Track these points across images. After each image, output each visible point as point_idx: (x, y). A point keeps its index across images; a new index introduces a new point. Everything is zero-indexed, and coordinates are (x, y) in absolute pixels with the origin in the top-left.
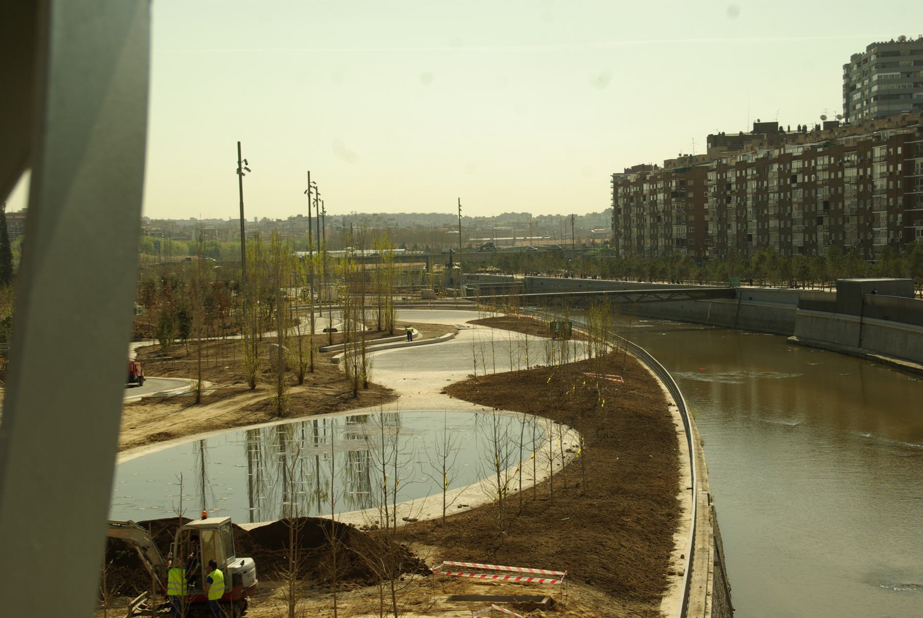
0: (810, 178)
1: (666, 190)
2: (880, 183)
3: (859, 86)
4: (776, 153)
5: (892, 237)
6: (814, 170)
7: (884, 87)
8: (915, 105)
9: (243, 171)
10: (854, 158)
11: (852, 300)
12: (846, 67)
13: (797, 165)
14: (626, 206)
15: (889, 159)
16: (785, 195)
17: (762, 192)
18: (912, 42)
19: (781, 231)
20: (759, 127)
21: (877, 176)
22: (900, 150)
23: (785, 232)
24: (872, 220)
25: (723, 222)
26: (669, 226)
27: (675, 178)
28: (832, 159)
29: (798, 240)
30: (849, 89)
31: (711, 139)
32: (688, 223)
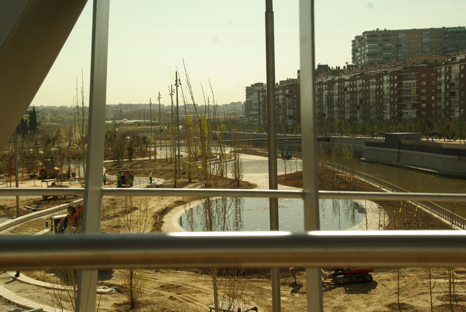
0: (353, 89)
1: (284, 94)
2: (386, 91)
3: (359, 50)
4: (337, 78)
5: (392, 115)
6: (355, 86)
7: (371, 50)
8: (384, 58)
9: (178, 84)
10: (374, 80)
11: (392, 142)
12: (353, 41)
13: (347, 83)
14: (264, 101)
15: (391, 81)
16: (341, 97)
17: (330, 96)
18: (381, 31)
19: (339, 112)
21: (385, 88)
22: (396, 77)
23: (342, 113)
24: (384, 108)
26: (285, 110)
27: (288, 89)
28: (364, 81)
29: (347, 116)
30: (354, 51)
32: (294, 109)
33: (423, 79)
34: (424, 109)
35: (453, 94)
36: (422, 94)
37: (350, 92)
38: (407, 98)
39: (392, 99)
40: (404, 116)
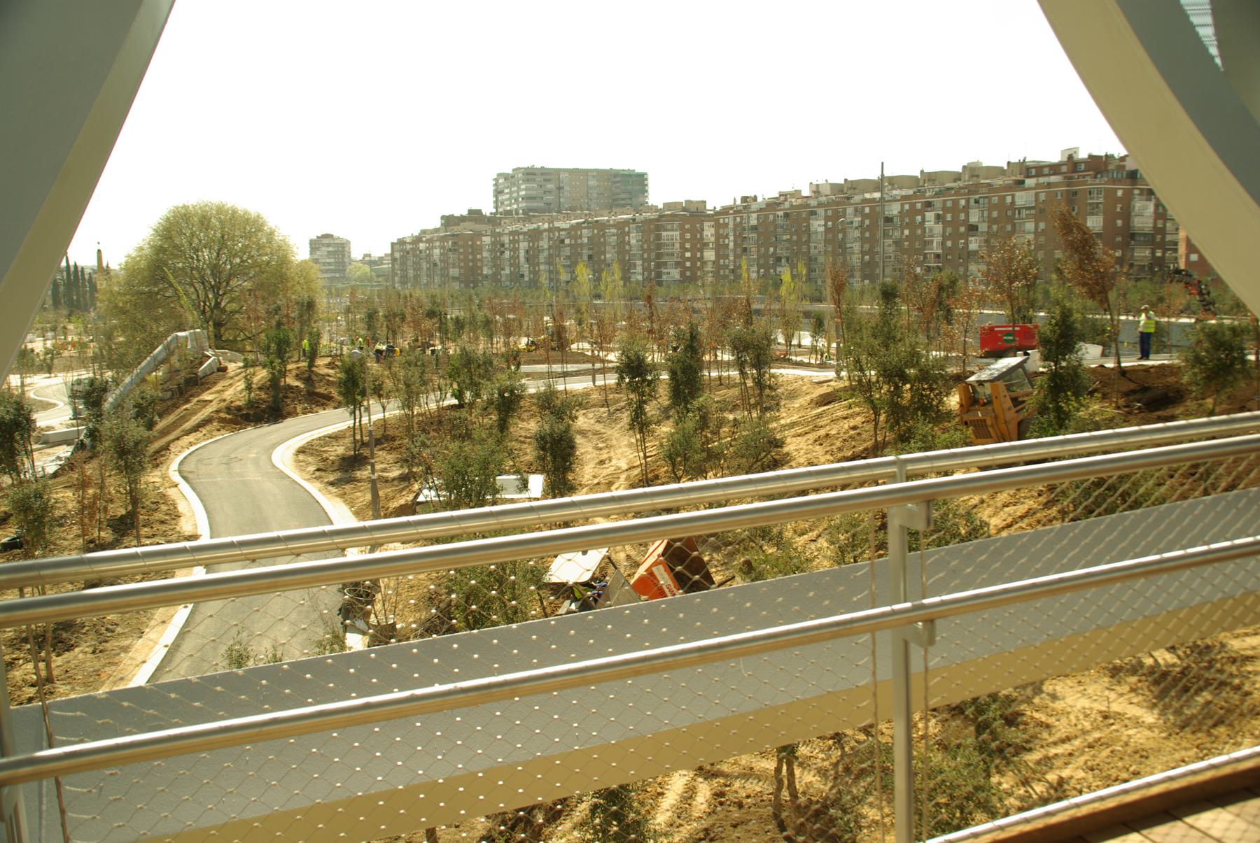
20: (470, 212)
25: (498, 267)
26: (445, 269)
30: (498, 192)
31: (443, 217)
32: (460, 268)
33: (688, 231)
37: (569, 245)
38: (668, 254)
39: (646, 256)
40: (664, 277)
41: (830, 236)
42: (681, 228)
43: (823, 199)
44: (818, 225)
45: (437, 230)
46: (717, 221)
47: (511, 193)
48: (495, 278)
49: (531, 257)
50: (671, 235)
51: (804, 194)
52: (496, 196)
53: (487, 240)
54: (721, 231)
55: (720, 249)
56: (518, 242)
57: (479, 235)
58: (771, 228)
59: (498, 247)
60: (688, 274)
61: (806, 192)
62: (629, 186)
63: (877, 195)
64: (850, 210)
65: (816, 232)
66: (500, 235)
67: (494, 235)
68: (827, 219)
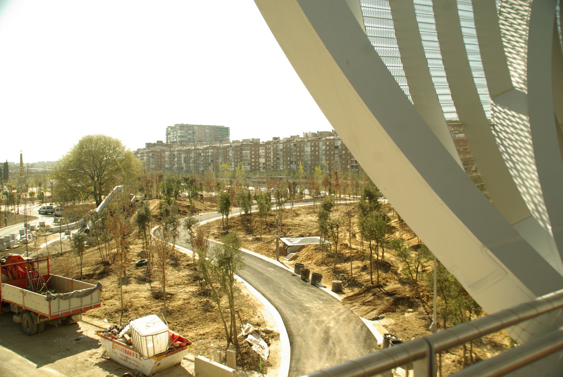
20: (158, 142)
30: (168, 134)
31: (146, 144)
33: (253, 151)
34: (253, 166)
35: (278, 158)
36: (253, 158)
37: (203, 156)
41: (313, 153)
42: (251, 149)
43: (310, 139)
44: (308, 149)
45: (144, 149)
46: (266, 147)
47: (173, 134)
48: (171, 169)
49: (187, 161)
50: (246, 152)
51: (300, 137)
52: (167, 136)
53: (167, 153)
54: (268, 151)
55: (267, 157)
56: (181, 154)
57: (164, 151)
58: (289, 150)
59: (172, 156)
60: (253, 168)
61: (302, 136)
62: (223, 132)
63: (332, 137)
64: (321, 144)
65: (307, 152)
66: (173, 151)
67: (170, 151)
68: (311, 146)
